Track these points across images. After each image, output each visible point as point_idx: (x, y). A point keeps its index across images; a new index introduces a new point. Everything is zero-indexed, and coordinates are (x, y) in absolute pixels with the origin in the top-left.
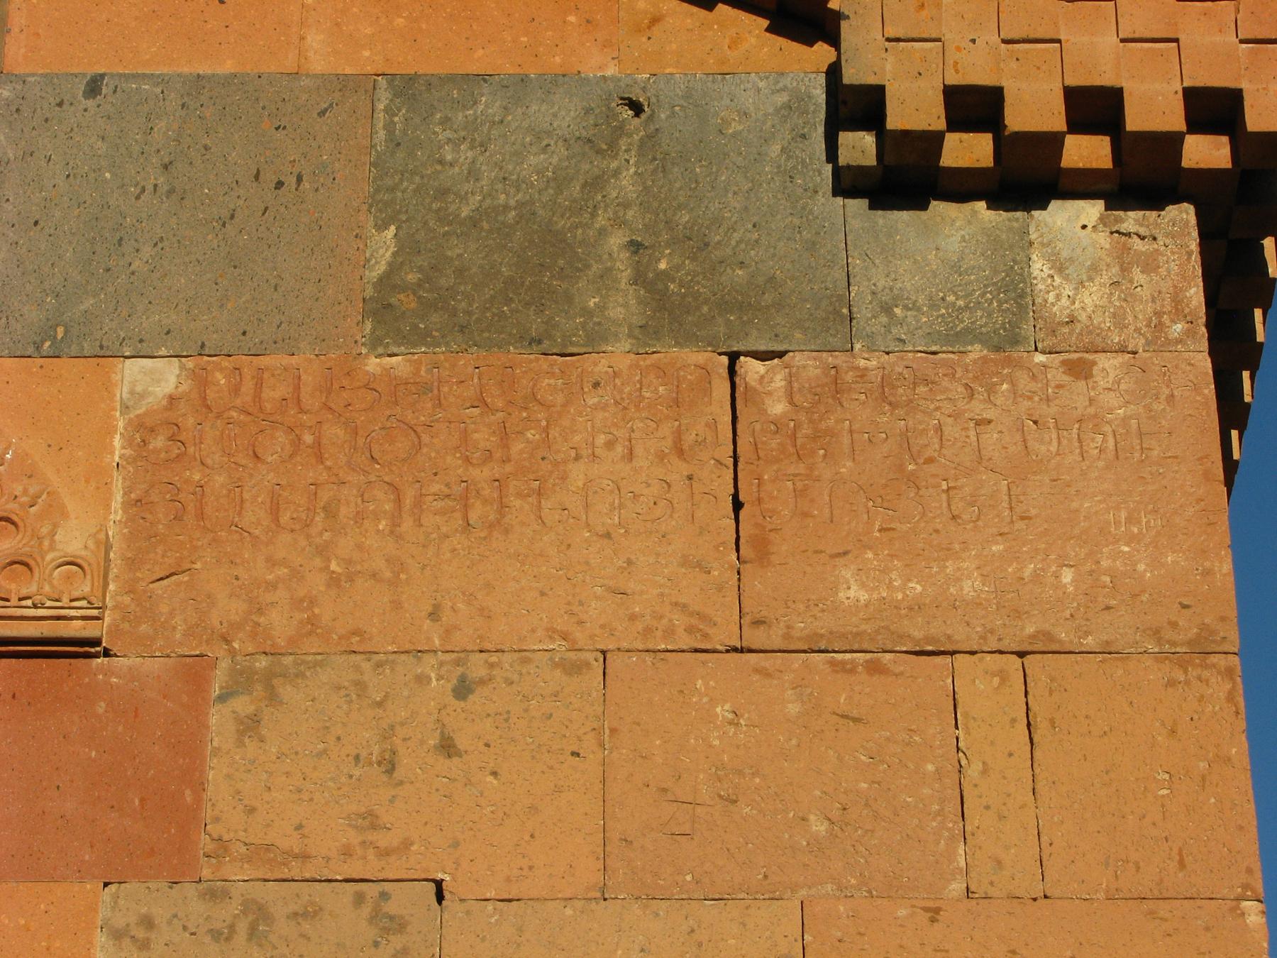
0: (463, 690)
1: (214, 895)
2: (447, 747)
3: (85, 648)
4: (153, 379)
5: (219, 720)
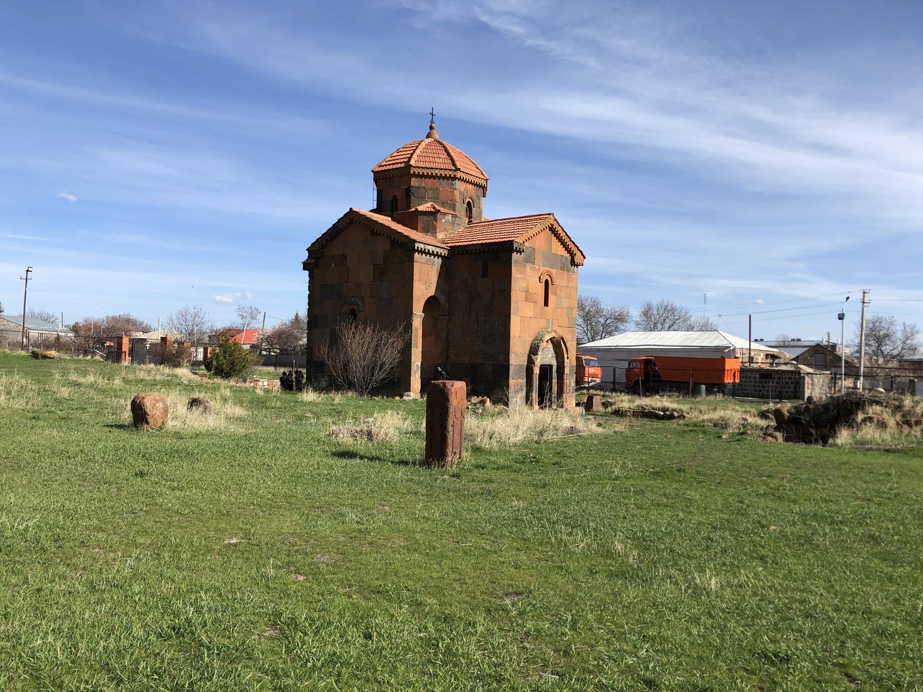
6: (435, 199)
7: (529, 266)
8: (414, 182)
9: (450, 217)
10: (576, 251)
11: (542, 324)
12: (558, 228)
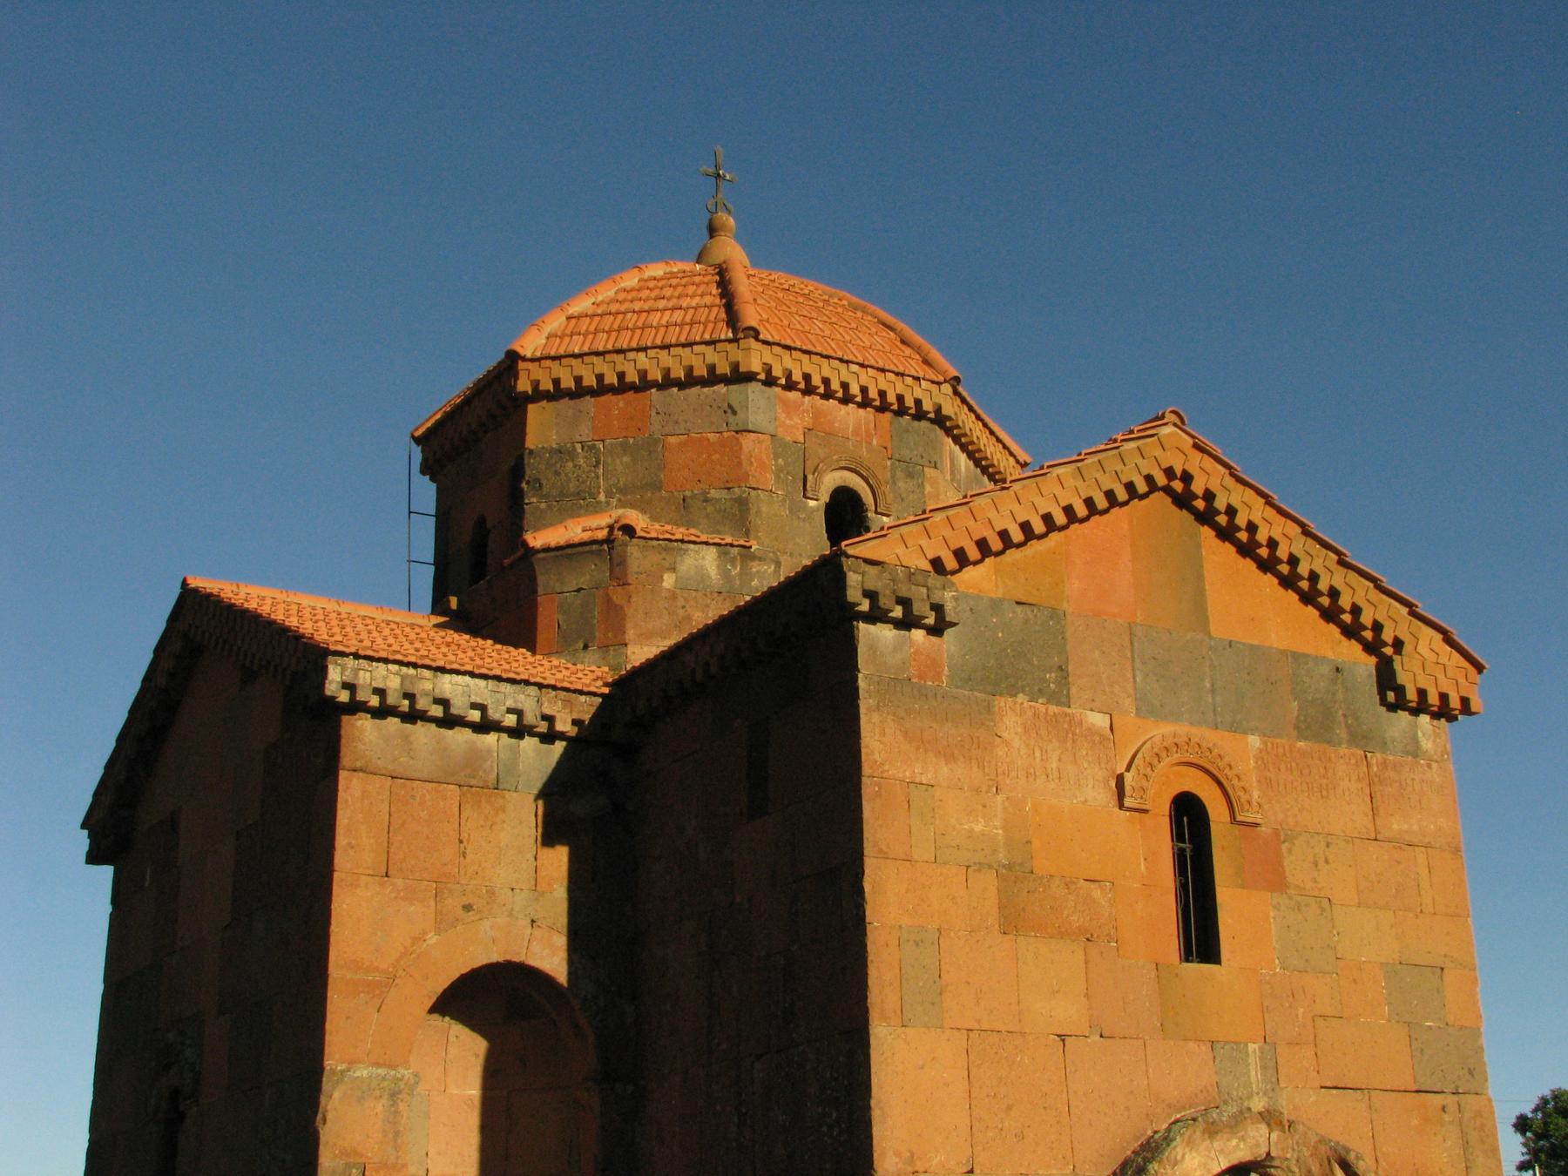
0: (1328, 846)
1: (1290, 898)
2: (1327, 862)
3: (1257, 825)
4: (1254, 741)
5: (1284, 847)
6: (642, 492)
7: (1013, 717)
8: (542, 427)
9: (708, 560)
10: (1396, 623)
11: (1182, 1073)
12: (1228, 495)
